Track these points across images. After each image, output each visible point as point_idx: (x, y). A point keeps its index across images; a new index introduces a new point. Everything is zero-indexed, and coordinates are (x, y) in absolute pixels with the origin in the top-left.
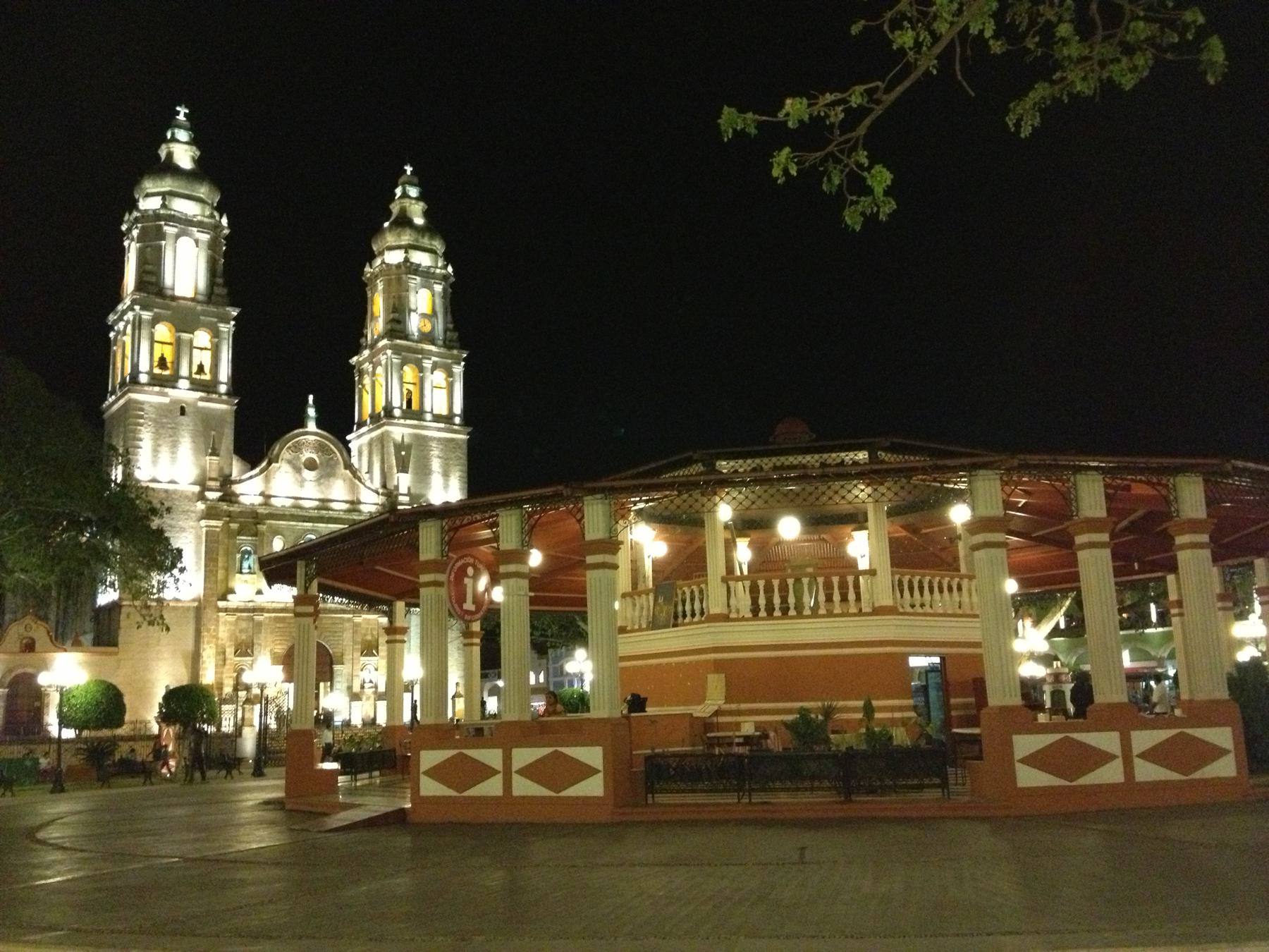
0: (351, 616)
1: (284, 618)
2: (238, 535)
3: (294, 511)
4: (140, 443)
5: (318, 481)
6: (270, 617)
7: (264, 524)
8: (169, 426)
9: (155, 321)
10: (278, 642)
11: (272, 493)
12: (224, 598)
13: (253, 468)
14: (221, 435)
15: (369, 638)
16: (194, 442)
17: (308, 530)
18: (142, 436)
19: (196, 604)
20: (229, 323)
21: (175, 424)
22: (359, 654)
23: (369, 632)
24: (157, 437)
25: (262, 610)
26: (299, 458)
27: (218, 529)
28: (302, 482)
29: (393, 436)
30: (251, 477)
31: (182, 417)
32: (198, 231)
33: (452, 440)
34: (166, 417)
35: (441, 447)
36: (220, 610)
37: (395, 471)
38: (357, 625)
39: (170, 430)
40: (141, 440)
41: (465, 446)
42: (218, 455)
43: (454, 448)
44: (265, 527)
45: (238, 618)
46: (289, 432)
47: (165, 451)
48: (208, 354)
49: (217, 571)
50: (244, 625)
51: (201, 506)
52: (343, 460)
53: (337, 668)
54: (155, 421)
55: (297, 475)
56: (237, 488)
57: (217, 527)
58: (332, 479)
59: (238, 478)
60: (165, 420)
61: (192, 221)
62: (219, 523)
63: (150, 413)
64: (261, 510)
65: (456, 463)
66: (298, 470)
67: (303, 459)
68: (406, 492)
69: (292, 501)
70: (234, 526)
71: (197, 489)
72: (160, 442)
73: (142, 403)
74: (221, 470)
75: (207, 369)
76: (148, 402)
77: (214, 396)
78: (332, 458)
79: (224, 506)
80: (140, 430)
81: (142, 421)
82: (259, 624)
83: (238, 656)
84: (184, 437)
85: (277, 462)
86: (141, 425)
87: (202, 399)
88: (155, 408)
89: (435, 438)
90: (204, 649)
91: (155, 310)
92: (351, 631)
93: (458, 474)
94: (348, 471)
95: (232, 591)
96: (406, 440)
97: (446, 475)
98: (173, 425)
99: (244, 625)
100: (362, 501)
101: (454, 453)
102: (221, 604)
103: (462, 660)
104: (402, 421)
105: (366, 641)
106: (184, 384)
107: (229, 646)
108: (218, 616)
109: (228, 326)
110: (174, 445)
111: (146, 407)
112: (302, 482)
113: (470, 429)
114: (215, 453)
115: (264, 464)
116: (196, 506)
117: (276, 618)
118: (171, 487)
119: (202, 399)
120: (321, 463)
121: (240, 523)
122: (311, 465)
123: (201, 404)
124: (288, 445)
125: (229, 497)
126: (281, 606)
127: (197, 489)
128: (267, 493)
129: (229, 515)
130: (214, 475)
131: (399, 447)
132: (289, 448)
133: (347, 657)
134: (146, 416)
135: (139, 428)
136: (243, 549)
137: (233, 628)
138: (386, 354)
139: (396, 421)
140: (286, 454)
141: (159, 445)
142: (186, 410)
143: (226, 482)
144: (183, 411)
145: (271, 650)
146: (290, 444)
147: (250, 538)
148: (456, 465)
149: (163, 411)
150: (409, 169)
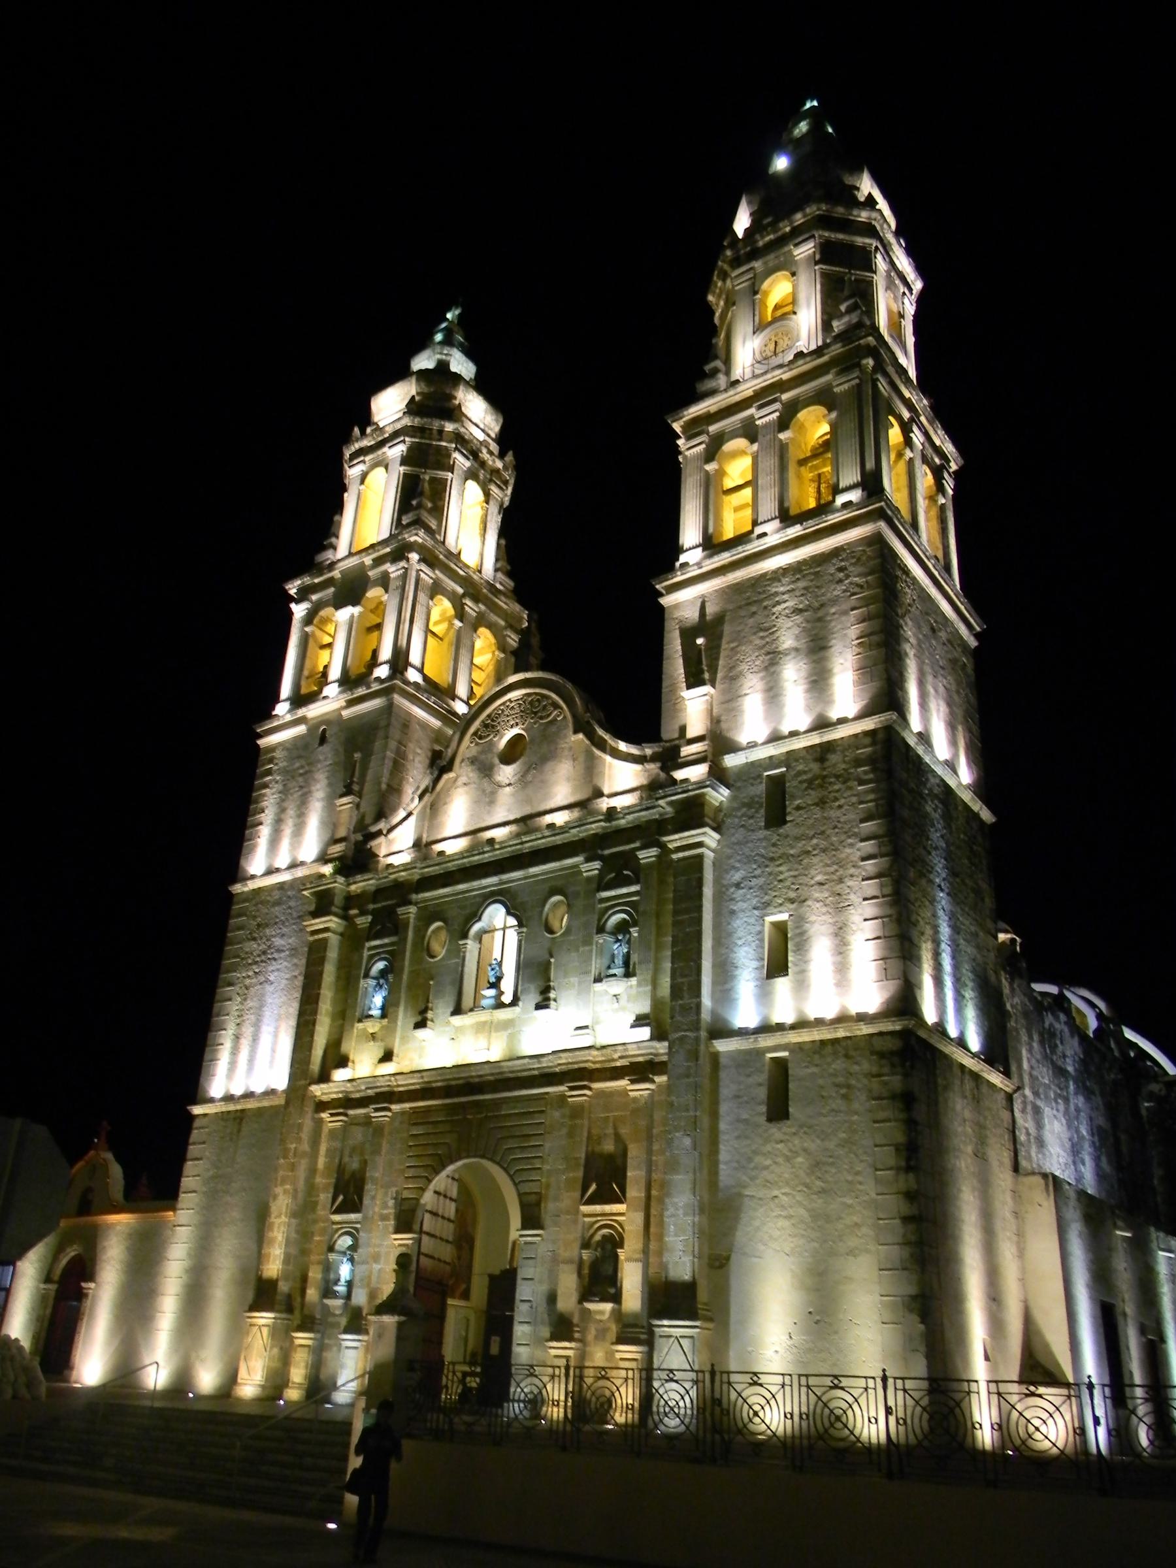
0: (562, 1088)
1: (428, 1110)
2: (369, 939)
6: (403, 1113)
7: (410, 903)
8: (301, 771)
10: (410, 1173)
15: (609, 1147)
16: (330, 785)
17: (493, 894)
21: (309, 764)
22: (578, 1194)
23: (610, 1131)
24: (285, 792)
25: (387, 1097)
26: (491, 744)
29: (677, 614)
32: (390, 447)
33: (836, 552)
34: (299, 757)
35: (801, 584)
36: (321, 1106)
38: (577, 1112)
39: (300, 779)
43: (841, 570)
44: (413, 909)
47: (291, 812)
52: (574, 716)
54: (284, 772)
55: (485, 783)
58: (549, 766)
60: (297, 765)
70: (363, 921)
72: (285, 804)
73: (272, 749)
76: (280, 744)
77: (361, 691)
78: (555, 720)
80: (264, 795)
82: (379, 1130)
83: (338, 1211)
84: (317, 781)
86: (266, 786)
87: (351, 703)
88: (288, 749)
89: (785, 571)
90: (275, 1197)
91: (314, 597)
92: (564, 1131)
93: (853, 631)
94: (581, 736)
95: (343, 1062)
96: (710, 610)
98: (307, 768)
99: (358, 1134)
101: (840, 581)
102: (318, 1090)
103: (894, 1204)
105: (601, 1155)
106: (332, 690)
107: (325, 1189)
111: (278, 754)
117: (415, 1111)
119: (351, 703)
120: (532, 741)
121: (374, 913)
124: (472, 729)
126: (414, 1082)
132: (475, 734)
137: (338, 1144)
142: (328, 732)
144: (323, 740)
145: (397, 1192)
146: (476, 725)
147: (386, 941)
148: (845, 613)
149: (298, 748)
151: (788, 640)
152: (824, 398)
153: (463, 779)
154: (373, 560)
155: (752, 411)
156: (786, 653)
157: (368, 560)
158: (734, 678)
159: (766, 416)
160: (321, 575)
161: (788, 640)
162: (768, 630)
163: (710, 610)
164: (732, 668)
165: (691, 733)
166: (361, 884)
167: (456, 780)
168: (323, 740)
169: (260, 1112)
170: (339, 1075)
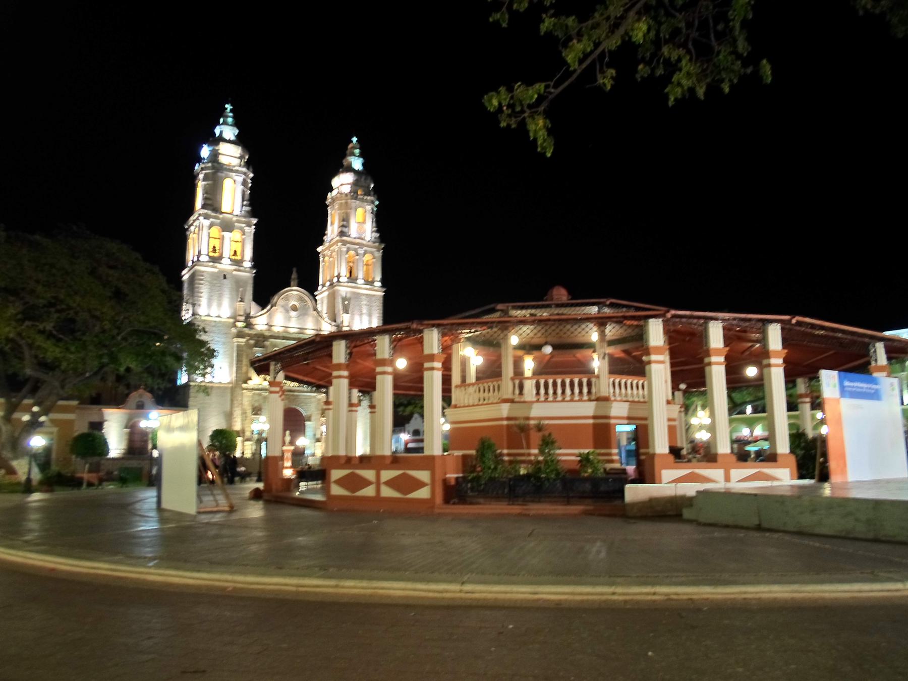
3: (285, 335)
4: (202, 295)
5: (298, 317)
7: (268, 341)
9: (211, 226)
11: (273, 324)
12: (246, 382)
13: (263, 309)
14: (245, 291)
18: (202, 291)
19: (230, 385)
20: (251, 227)
24: (211, 291)
26: (287, 305)
27: (242, 344)
28: (289, 318)
30: (261, 315)
31: (225, 280)
33: (374, 295)
34: (216, 280)
37: (341, 312)
40: (202, 293)
41: (382, 299)
42: (243, 302)
45: (254, 394)
46: (282, 289)
48: (240, 245)
49: (242, 367)
50: (257, 398)
51: (234, 330)
53: (307, 423)
54: (210, 283)
56: (254, 321)
57: (242, 342)
58: (306, 316)
59: (254, 315)
60: (214, 282)
61: (232, 170)
62: (244, 340)
63: (207, 278)
64: (267, 334)
65: (377, 308)
66: (287, 311)
67: (291, 305)
68: (347, 325)
69: (284, 328)
70: (252, 342)
71: (232, 320)
73: (203, 272)
74: (245, 310)
75: (238, 253)
79: (247, 331)
80: (201, 287)
81: (202, 282)
83: (254, 415)
85: (275, 306)
86: (202, 284)
87: (235, 270)
90: (235, 411)
91: (211, 220)
93: (377, 315)
97: (370, 315)
99: (257, 398)
100: (322, 329)
102: (244, 386)
104: (346, 284)
107: (249, 409)
108: (242, 393)
109: (250, 229)
110: (220, 296)
111: (204, 274)
112: (289, 318)
113: (384, 290)
114: (242, 301)
115: (269, 307)
116: (231, 330)
118: (218, 319)
119: (235, 270)
122: (294, 308)
123: (235, 273)
125: (249, 325)
127: (232, 320)
128: (270, 324)
129: (249, 335)
130: (242, 314)
131: (344, 299)
133: (313, 418)
134: (205, 279)
135: (201, 286)
136: (257, 355)
138: (337, 245)
139: (342, 284)
140: (281, 302)
141: (212, 296)
143: (248, 317)
146: (282, 296)
150: (355, 139)
151: (364, 311)
152: (372, 253)
153: (279, 311)
154: (236, 220)
155: (357, 247)
156: (364, 314)
157: (235, 219)
158: (353, 315)
159: (361, 251)
160: (216, 213)
161: (364, 311)
162: (360, 307)
163: (348, 296)
164: (353, 312)
165: (344, 325)
166: (252, 332)
167: (277, 309)
168: (225, 277)
169: (219, 388)
170: (249, 382)
